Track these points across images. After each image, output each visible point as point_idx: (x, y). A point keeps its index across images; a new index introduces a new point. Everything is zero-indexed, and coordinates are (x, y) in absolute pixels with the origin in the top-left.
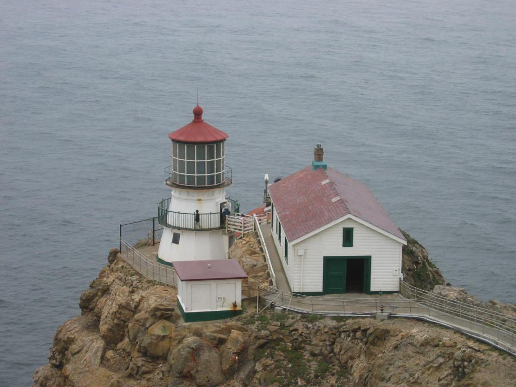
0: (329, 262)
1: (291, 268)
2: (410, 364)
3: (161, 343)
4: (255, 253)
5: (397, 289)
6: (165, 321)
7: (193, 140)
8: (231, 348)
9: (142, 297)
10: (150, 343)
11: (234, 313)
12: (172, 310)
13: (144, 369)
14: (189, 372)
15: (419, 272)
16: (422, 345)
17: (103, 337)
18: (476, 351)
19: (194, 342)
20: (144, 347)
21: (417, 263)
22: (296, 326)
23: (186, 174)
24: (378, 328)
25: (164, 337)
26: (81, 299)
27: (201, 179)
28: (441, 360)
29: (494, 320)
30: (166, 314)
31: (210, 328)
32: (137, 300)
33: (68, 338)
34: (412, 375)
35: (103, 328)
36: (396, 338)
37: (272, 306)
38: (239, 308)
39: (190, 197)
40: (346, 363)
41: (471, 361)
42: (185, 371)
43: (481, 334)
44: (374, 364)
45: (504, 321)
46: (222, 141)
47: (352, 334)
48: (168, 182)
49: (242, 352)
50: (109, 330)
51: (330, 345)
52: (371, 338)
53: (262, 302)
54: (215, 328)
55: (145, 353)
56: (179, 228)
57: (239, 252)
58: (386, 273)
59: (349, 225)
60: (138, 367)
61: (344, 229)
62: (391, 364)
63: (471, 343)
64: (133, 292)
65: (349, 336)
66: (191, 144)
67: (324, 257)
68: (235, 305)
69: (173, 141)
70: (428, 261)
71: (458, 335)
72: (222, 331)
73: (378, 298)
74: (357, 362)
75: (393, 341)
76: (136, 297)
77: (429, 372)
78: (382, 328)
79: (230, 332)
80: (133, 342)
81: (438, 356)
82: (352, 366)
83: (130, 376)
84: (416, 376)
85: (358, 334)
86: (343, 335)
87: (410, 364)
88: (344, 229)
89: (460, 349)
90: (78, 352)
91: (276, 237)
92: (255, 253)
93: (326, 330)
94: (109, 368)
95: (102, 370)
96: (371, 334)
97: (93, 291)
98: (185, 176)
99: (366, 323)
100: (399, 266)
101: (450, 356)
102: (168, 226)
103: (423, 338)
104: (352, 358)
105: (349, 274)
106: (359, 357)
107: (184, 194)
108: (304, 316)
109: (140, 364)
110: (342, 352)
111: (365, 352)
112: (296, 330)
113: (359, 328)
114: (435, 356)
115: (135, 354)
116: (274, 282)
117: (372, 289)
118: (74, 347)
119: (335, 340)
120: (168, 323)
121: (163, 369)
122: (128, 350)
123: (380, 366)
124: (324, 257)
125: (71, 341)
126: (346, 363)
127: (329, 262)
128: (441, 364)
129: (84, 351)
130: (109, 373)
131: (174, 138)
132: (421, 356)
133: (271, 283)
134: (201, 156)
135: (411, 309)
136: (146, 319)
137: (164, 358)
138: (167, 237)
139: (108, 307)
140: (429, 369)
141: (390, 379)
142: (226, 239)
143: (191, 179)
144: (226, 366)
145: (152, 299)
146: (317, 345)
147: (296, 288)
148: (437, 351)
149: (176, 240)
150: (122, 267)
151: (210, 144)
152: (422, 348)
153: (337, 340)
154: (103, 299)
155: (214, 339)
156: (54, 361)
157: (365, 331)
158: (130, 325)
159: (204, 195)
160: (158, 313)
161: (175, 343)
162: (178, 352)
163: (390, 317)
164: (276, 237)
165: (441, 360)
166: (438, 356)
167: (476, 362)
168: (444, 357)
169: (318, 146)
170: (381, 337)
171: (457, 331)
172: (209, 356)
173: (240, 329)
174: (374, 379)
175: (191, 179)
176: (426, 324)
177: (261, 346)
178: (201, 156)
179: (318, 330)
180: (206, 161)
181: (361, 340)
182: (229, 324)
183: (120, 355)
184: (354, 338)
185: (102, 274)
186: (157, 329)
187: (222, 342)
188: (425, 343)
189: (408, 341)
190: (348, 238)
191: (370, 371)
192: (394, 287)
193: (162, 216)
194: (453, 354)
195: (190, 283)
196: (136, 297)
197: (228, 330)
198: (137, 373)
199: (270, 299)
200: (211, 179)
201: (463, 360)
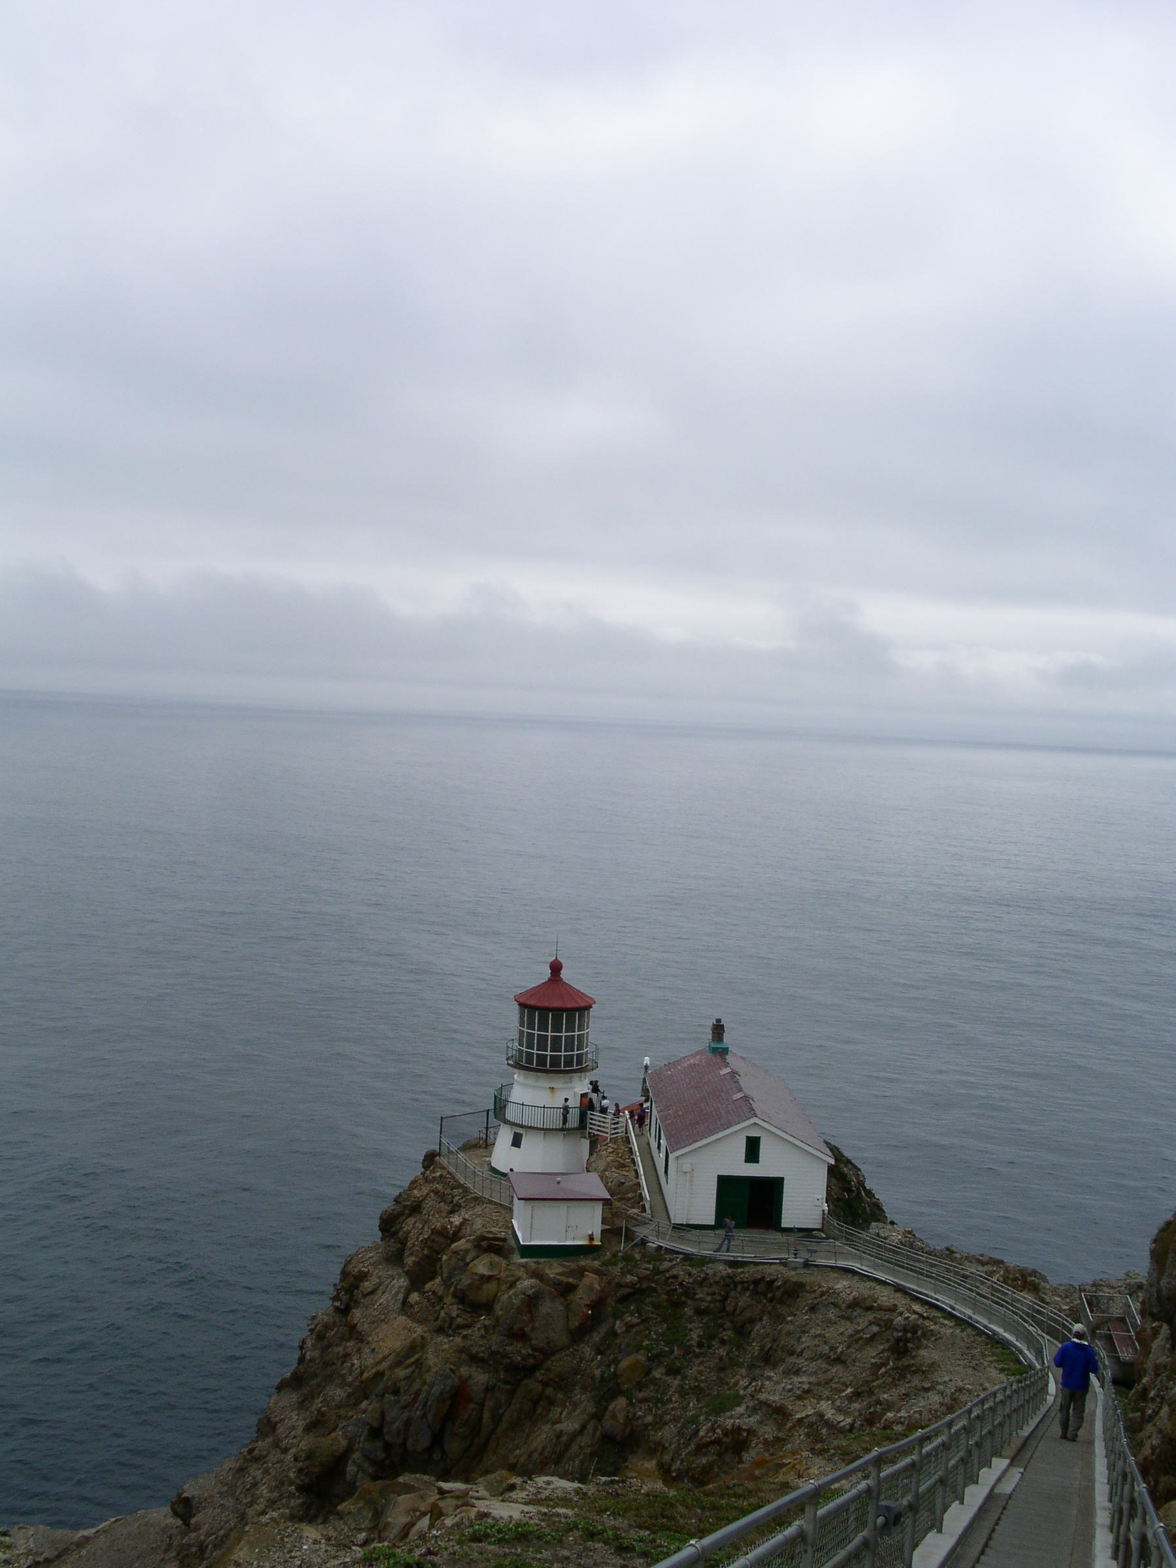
0: (725, 1183)
1: (672, 1189)
2: (831, 1333)
3: (485, 1286)
4: (624, 1166)
5: (819, 1226)
6: (493, 1255)
7: (546, 1004)
8: (581, 1299)
9: (465, 1220)
10: (470, 1285)
11: (588, 1250)
12: (504, 1240)
13: (459, 1320)
14: (522, 1329)
16: (849, 1306)
17: (407, 1273)
18: (924, 1318)
19: (532, 1287)
20: (461, 1290)
21: (849, 1191)
22: (674, 1272)
24: (788, 1281)
25: (490, 1278)
26: (381, 1218)
28: (875, 1329)
30: (497, 1246)
31: (554, 1269)
32: (457, 1223)
33: (360, 1271)
34: (832, 1348)
35: (410, 1261)
36: (813, 1296)
37: (643, 1242)
38: (597, 1242)
39: (538, 1084)
40: (742, 1326)
41: (916, 1332)
42: (517, 1326)
43: (932, 1294)
44: (781, 1330)
45: (965, 1277)
47: (751, 1287)
48: (511, 1062)
49: (597, 1305)
50: (416, 1263)
51: (719, 1301)
52: (778, 1294)
53: (630, 1236)
54: (560, 1270)
55: (461, 1298)
56: (522, 1126)
57: (601, 1164)
58: (805, 1201)
59: (754, 1133)
60: (452, 1319)
62: (804, 1332)
63: (917, 1307)
64: (452, 1212)
65: (748, 1289)
67: (719, 1177)
68: (591, 1238)
69: (522, 1006)
70: (864, 1188)
71: (898, 1295)
72: (571, 1273)
74: (758, 1327)
75: (809, 1299)
76: (456, 1220)
77: (857, 1346)
78: (794, 1280)
79: (583, 1275)
80: (447, 1284)
81: (871, 1323)
82: (750, 1333)
83: (440, 1330)
84: (839, 1350)
85: (762, 1287)
86: (739, 1288)
87: (831, 1333)
89: (901, 1314)
90: (372, 1293)
91: (654, 1145)
92: (624, 1166)
93: (717, 1279)
94: (412, 1317)
95: (402, 1319)
96: (779, 1287)
97: (398, 1208)
99: (771, 1271)
100: (822, 1194)
101: (888, 1325)
102: (507, 1122)
103: (851, 1297)
104: (751, 1321)
105: (751, 1202)
106: (761, 1319)
107: (532, 1079)
108: (688, 1257)
109: (454, 1314)
110: (738, 1312)
111: (770, 1313)
112: (675, 1277)
113: (763, 1278)
114: (866, 1323)
115: (449, 1299)
116: (647, 1207)
117: (783, 1225)
118: (367, 1285)
119: (728, 1293)
120: (497, 1259)
121: (486, 1323)
122: (440, 1293)
123: (789, 1334)
124: (719, 1177)
125: (363, 1276)
126: (742, 1326)
127: (725, 1183)
128: (874, 1335)
129: (380, 1292)
130: (410, 1323)
131: (522, 1000)
132: (848, 1323)
133: (644, 1210)
134: (557, 1028)
135: (836, 1254)
136: (467, 1251)
137: (488, 1307)
138: (504, 1137)
139: (415, 1230)
140: (857, 1341)
141: (802, 1352)
142: (586, 1144)
143: (542, 1060)
144: (574, 1324)
145: (478, 1221)
146: (702, 1300)
147: (678, 1218)
148: (871, 1316)
149: (517, 1142)
150: (441, 1176)
151: (571, 1011)
152: (849, 1311)
153: (732, 1294)
154: (411, 1221)
155: (560, 1283)
156: (338, 1304)
157: (772, 1282)
158: (445, 1258)
160: (484, 1244)
161: (504, 1287)
162: (509, 1299)
163: (806, 1264)
164: (654, 1145)
165: (875, 1329)
166: (871, 1323)
167: (924, 1335)
168: (879, 1325)
169: (719, 1021)
170: (794, 1291)
171: (899, 1289)
172: (550, 1307)
173: (596, 1272)
174: (779, 1352)
175: (542, 1060)
176: (856, 1277)
177: (625, 1299)
178: (557, 1028)
179: (705, 1279)
180: (564, 1034)
181: (765, 1296)
182: (582, 1263)
183: (429, 1300)
184: (755, 1292)
185: (414, 1184)
186: (481, 1267)
187: (571, 1288)
188: (855, 1304)
189: (829, 1299)
190: (753, 1150)
191: (775, 1341)
193: (500, 1106)
194: (892, 1321)
195: (532, 1203)
196: (456, 1220)
197: (580, 1273)
198: (450, 1327)
199: (641, 1232)
200: (569, 1062)
201: (905, 1331)
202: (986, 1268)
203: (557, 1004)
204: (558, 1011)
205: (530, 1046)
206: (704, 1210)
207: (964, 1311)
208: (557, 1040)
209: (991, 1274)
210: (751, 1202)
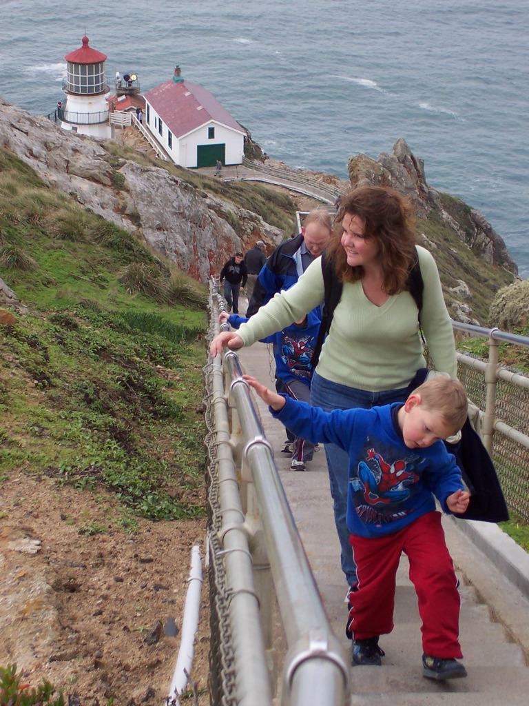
0: (202, 150)
5: (241, 162)
15: (252, 151)
23: (80, 85)
27: (91, 89)
29: (303, 180)
39: (83, 101)
46: (102, 62)
56: (77, 124)
58: (234, 154)
59: (212, 126)
61: (209, 128)
66: (83, 65)
67: (198, 146)
71: (284, 189)
73: (234, 169)
88: (209, 128)
91: (155, 131)
92: (142, 142)
98: (79, 87)
105: (211, 155)
107: (79, 98)
117: (226, 163)
124: (198, 146)
127: (202, 150)
134: (90, 73)
143: (77, 88)
151: (97, 64)
159: (93, 99)
164: (155, 131)
169: (177, 67)
171: (284, 187)
175: (84, 89)
192: (240, 161)
202: (316, 176)
203: (90, 61)
204: (90, 64)
205: (77, 82)
206: (191, 160)
207: (309, 193)
208: (91, 80)
209: (317, 178)
210: (211, 155)
